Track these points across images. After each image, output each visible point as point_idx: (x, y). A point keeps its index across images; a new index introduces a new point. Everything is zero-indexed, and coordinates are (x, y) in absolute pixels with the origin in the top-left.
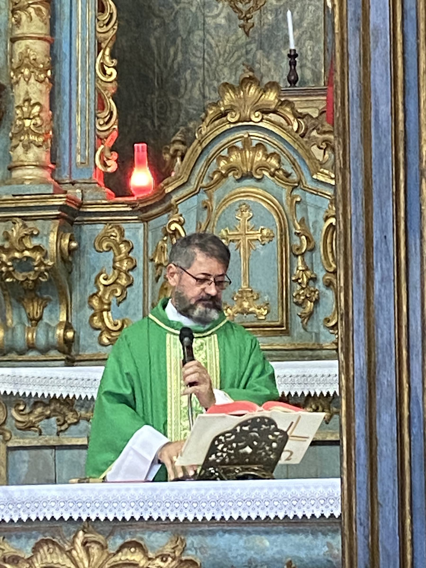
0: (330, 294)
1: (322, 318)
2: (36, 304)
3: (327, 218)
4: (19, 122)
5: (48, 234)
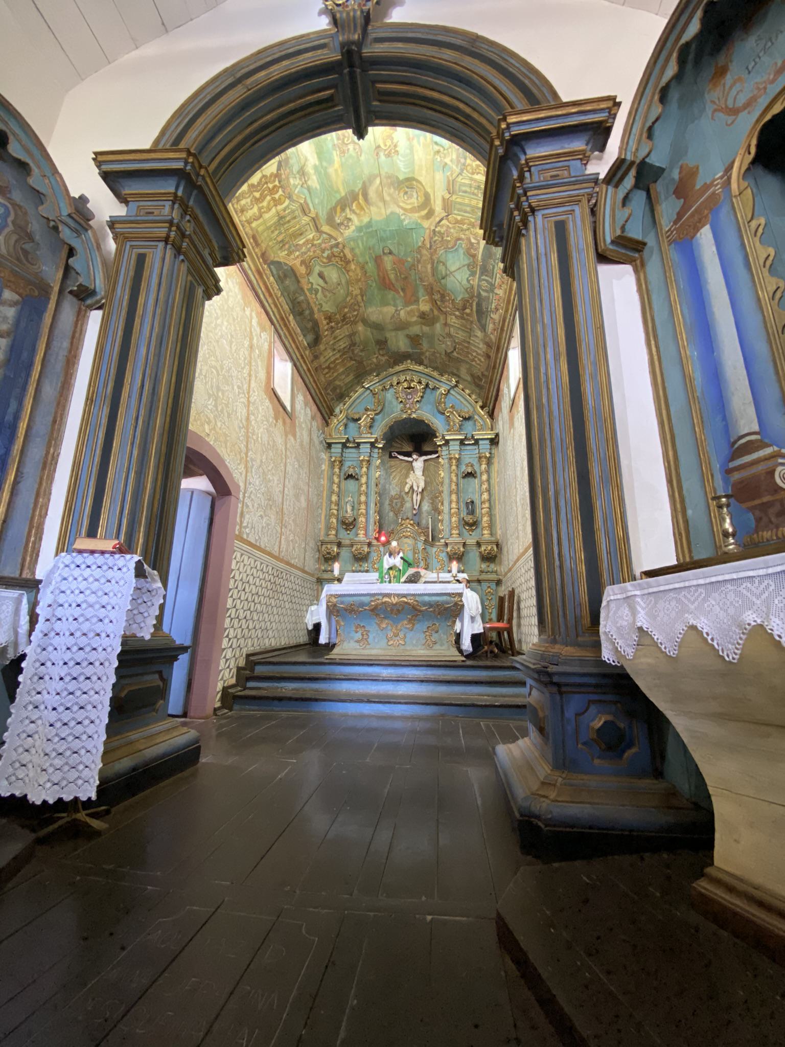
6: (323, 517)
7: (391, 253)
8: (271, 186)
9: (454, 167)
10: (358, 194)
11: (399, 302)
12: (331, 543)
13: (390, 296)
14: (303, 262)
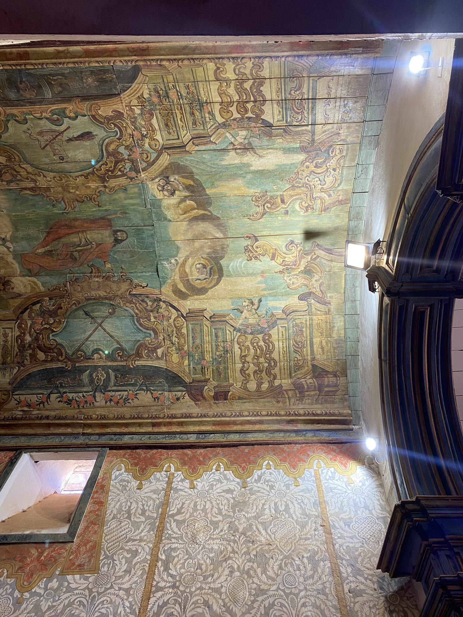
7: (117, 241)
8: (249, 106)
9: (240, 322)
10: (206, 210)
11: (24, 246)
13: (32, 232)
14: (119, 115)
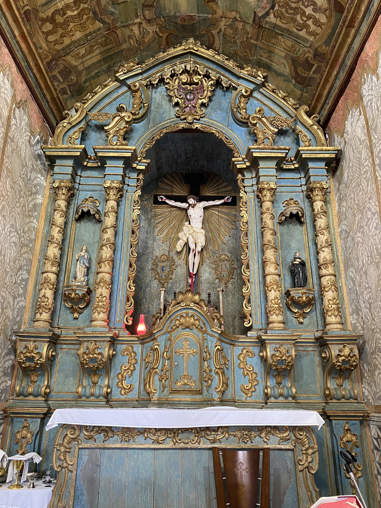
0: (217, 377)
1: (214, 387)
2: (96, 377)
3: (216, 346)
4: (97, 303)
5: (105, 348)
6: (30, 287)
12: (37, 337)
